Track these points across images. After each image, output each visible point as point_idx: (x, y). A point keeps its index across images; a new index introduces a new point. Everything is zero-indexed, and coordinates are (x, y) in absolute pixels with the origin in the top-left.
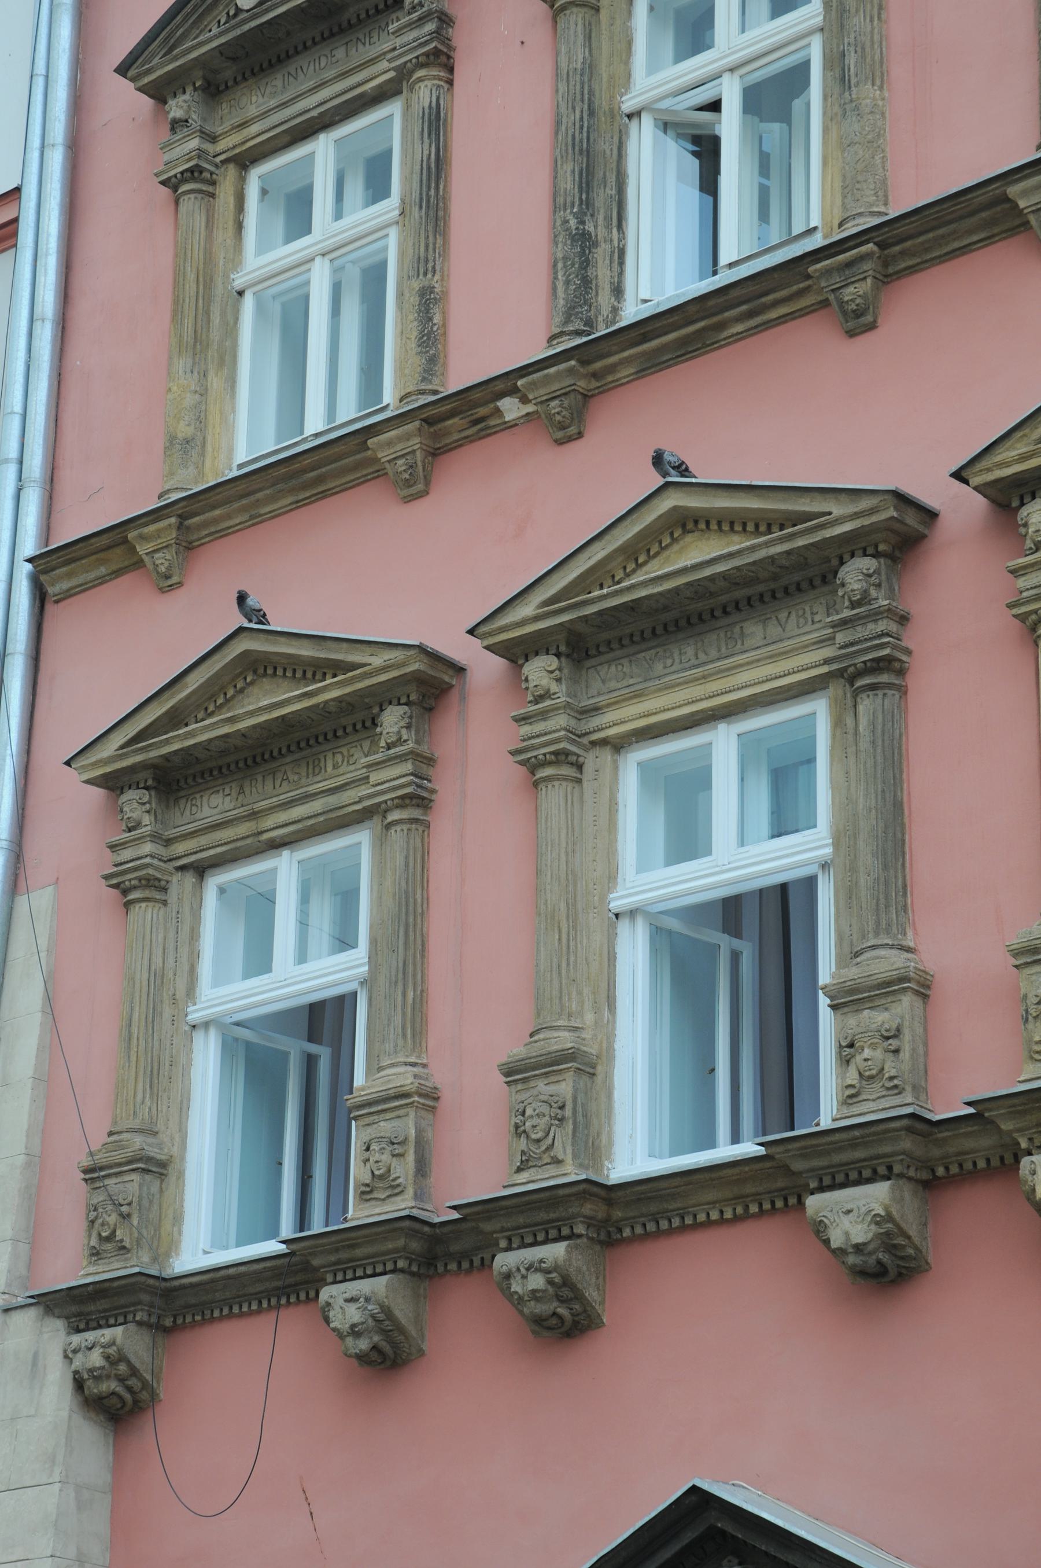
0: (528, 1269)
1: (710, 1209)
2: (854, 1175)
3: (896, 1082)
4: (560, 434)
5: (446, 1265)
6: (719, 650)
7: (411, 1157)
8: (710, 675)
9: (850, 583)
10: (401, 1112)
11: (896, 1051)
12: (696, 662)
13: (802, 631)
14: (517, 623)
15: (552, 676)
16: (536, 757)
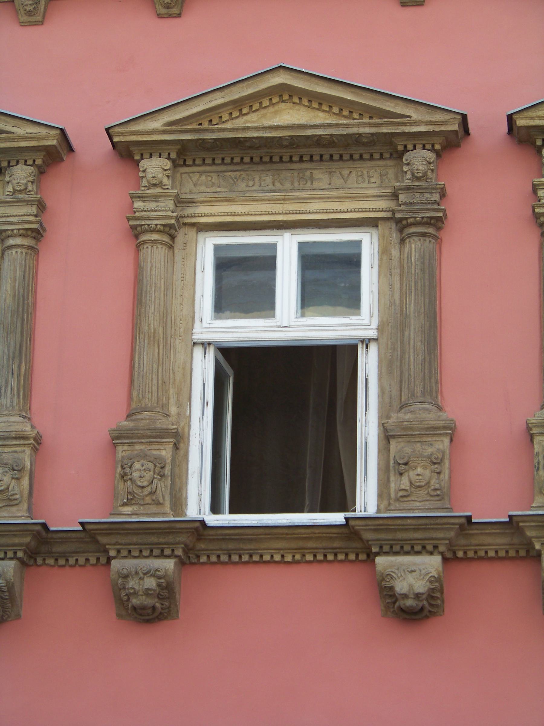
0: (145, 574)
1: (275, 553)
2: (407, 548)
3: (438, 492)
4: (163, 11)
5: (44, 560)
6: (292, 184)
7: (25, 482)
8: (289, 199)
9: (416, 165)
10: (19, 449)
11: (439, 473)
12: (274, 188)
13: (360, 186)
14: (147, 132)
15: (165, 173)
16: (149, 225)
